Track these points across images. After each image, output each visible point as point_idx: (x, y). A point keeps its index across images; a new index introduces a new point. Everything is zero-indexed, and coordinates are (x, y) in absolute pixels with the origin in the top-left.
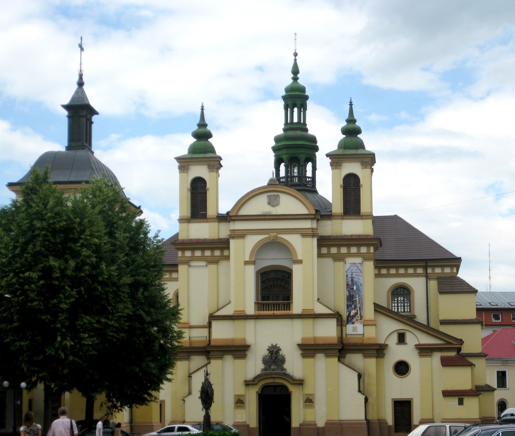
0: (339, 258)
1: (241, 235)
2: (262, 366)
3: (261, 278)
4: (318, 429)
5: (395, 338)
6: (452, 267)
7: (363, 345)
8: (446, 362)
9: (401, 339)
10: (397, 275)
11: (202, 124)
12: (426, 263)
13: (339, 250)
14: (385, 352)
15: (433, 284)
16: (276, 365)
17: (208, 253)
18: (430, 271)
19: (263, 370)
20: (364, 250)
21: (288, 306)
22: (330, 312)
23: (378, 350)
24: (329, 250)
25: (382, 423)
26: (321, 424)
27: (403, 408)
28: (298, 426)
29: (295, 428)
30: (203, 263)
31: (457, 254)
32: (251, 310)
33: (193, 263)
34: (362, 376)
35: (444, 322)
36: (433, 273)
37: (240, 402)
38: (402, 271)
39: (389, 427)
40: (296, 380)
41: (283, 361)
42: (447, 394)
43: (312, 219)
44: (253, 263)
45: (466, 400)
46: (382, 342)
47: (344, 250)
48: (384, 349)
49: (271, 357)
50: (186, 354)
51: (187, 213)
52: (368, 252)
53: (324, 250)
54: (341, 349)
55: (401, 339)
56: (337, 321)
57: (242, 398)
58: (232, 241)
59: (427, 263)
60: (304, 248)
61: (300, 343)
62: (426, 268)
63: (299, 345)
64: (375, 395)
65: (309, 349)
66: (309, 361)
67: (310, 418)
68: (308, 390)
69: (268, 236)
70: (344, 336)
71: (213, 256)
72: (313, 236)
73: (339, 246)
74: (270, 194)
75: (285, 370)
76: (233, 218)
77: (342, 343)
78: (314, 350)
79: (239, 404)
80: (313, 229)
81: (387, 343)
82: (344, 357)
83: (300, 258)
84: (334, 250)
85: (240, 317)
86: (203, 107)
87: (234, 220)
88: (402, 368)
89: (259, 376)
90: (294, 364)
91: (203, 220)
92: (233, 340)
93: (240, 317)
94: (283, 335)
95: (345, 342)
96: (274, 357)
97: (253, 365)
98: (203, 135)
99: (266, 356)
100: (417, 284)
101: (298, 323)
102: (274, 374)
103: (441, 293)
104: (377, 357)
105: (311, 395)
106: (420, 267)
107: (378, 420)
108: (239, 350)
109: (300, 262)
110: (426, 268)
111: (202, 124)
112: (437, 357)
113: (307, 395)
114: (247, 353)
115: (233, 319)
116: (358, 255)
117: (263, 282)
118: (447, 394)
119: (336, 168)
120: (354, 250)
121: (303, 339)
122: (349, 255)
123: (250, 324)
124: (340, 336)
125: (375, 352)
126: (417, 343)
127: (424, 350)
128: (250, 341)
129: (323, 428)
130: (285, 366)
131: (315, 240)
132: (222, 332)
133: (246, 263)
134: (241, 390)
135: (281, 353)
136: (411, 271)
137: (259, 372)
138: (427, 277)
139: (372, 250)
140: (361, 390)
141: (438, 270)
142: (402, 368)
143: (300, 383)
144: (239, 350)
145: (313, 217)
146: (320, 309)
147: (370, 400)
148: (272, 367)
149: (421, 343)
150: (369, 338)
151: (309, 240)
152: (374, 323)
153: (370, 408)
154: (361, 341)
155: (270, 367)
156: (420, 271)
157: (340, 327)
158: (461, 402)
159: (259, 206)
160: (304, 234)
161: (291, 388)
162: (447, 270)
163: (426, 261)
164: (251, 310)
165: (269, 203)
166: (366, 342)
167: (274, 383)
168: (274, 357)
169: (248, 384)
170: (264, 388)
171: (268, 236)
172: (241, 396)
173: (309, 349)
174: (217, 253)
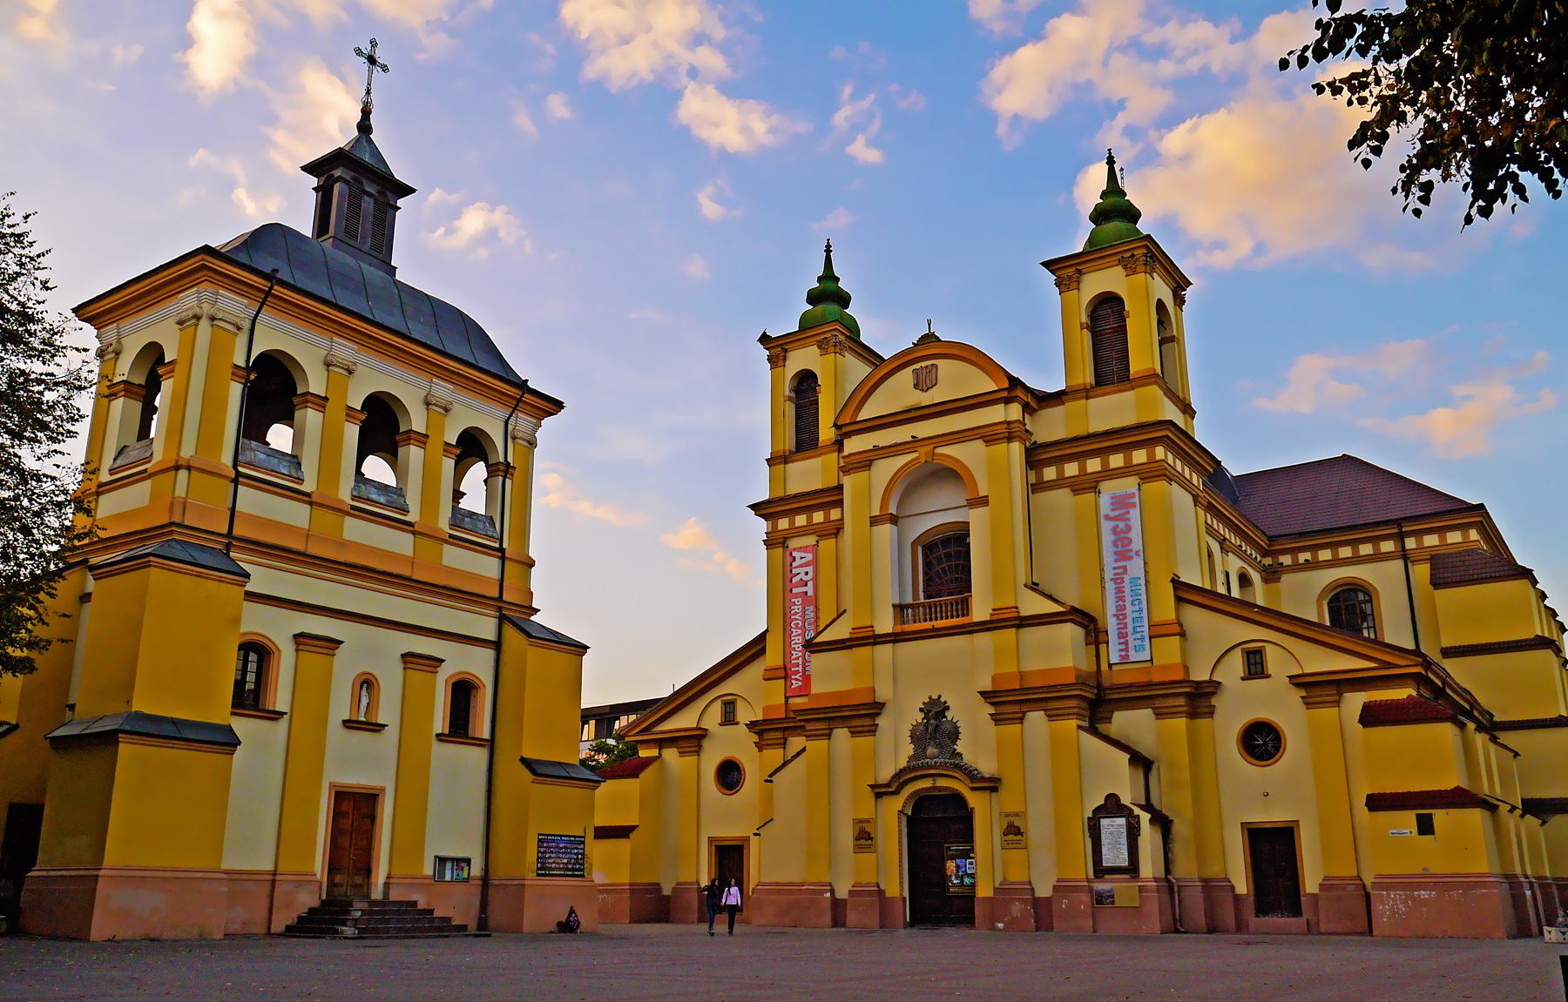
0: (1087, 485)
1: (863, 462)
2: (909, 749)
3: (925, 556)
4: (1037, 903)
5: (1237, 662)
6: (1463, 527)
7: (1149, 685)
8: (1373, 716)
9: (1255, 665)
10: (1337, 562)
11: (829, 275)
12: (1398, 528)
13: (1082, 468)
14: (1214, 701)
15: (1422, 572)
16: (939, 746)
17: (818, 517)
18: (1410, 543)
19: (911, 759)
20: (1139, 456)
21: (964, 607)
22: (1061, 609)
23: (1199, 698)
24: (1060, 472)
25: (1213, 888)
26: (1044, 890)
27: (1273, 848)
28: (990, 894)
29: (984, 899)
30: (810, 540)
31: (1474, 500)
32: (885, 624)
33: (794, 543)
34: (1154, 767)
35: (1448, 652)
36: (1421, 548)
37: (864, 837)
38: (1345, 552)
39: (1237, 899)
40: (983, 779)
41: (954, 735)
42: (1377, 802)
43: (1007, 401)
44: (894, 520)
45: (1440, 817)
46: (1201, 674)
47: (1094, 465)
48: (1213, 694)
49: (926, 726)
50: (779, 734)
51: (789, 443)
52: (1152, 460)
53: (1050, 473)
54: (1096, 702)
55: (1255, 665)
56: (1087, 634)
57: (868, 828)
58: (847, 481)
59: (1400, 527)
60: (997, 467)
61: (988, 687)
62: (1400, 537)
63: (982, 693)
64: (1188, 813)
65: (1008, 702)
66: (1014, 728)
67: (1017, 876)
68: (1008, 800)
69: (915, 455)
70: (1104, 667)
71: (827, 520)
72: (1009, 439)
73: (1081, 457)
74: (917, 366)
75: (960, 755)
76: (845, 429)
77: (1099, 686)
78: (1021, 702)
79: (863, 842)
80: (1009, 423)
81: (1216, 678)
82: (1109, 720)
83: (982, 494)
84: (1071, 469)
85: (866, 639)
86: (828, 246)
87: (848, 435)
88: (1261, 741)
89: (902, 772)
90: (979, 742)
91: (812, 453)
92: (849, 693)
93: (866, 639)
94: (956, 671)
95: (1106, 683)
96: (936, 727)
97: (893, 747)
98: (828, 294)
99: (918, 724)
100: (1383, 578)
101: (983, 640)
102: (931, 767)
103: (1437, 583)
104: (1193, 715)
105: (1016, 815)
106: (1385, 538)
107: (1202, 880)
108: (862, 714)
109: (983, 501)
110: (1400, 537)
111: (829, 275)
112: (1355, 701)
113: (1008, 815)
114: (879, 721)
115: (850, 647)
116: (1126, 471)
117: (927, 566)
118: (1377, 802)
119: (1069, 289)
120: (1116, 461)
121: (994, 678)
122: (1108, 474)
123: (884, 651)
124: (1094, 668)
125: (1182, 701)
126: (1299, 672)
127: (1318, 689)
128: (884, 693)
129: (1048, 900)
130: (959, 747)
131: (1016, 449)
132: (831, 677)
133: (874, 521)
134: (867, 807)
135: (949, 715)
136: (1366, 549)
137: (903, 764)
138: (1405, 556)
139: (1160, 452)
140: (1154, 800)
141: (1431, 540)
142: (1261, 741)
143: (992, 785)
144: (862, 714)
145: (1005, 394)
146: (1034, 605)
147: (1179, 828)
148: (931, 750)
149: (1307, 671)
150: (1165, 668)
151: (1003, 446)
152: (1177, 629)
153: (1177, 847)
154: (1144, 679)
155: (924, 750)
156: (1388, 546)
157: (1093, 647)
158: (1425, 826)
159: (898, 393)
160: (989, 435)
161: (975, 800)
162: (1454, 537)
163: (1398, 522)
164: (885, 624)
165: (916, 386)
166: (1156, 678)
167: (934, 788)
168: (936, 727)
169: (880, 792)
170: (921, 802)
171: (915, 455)
172: (868, 821)
173: (1008, 702)
174: (835, 514)
